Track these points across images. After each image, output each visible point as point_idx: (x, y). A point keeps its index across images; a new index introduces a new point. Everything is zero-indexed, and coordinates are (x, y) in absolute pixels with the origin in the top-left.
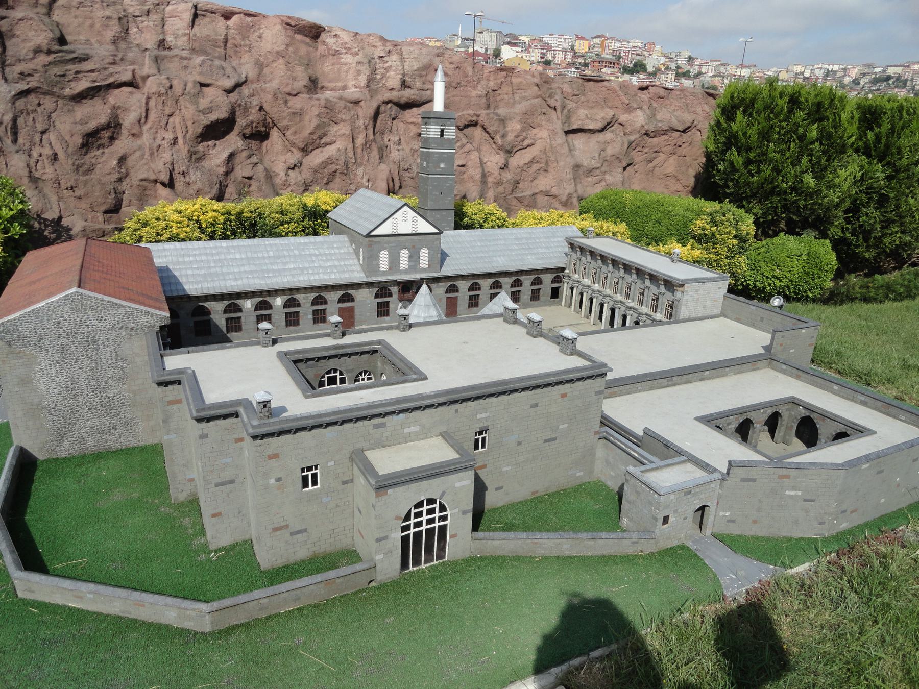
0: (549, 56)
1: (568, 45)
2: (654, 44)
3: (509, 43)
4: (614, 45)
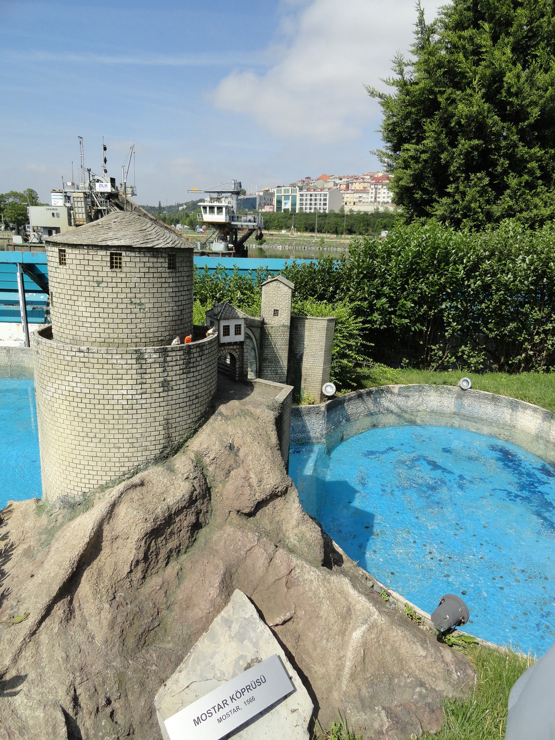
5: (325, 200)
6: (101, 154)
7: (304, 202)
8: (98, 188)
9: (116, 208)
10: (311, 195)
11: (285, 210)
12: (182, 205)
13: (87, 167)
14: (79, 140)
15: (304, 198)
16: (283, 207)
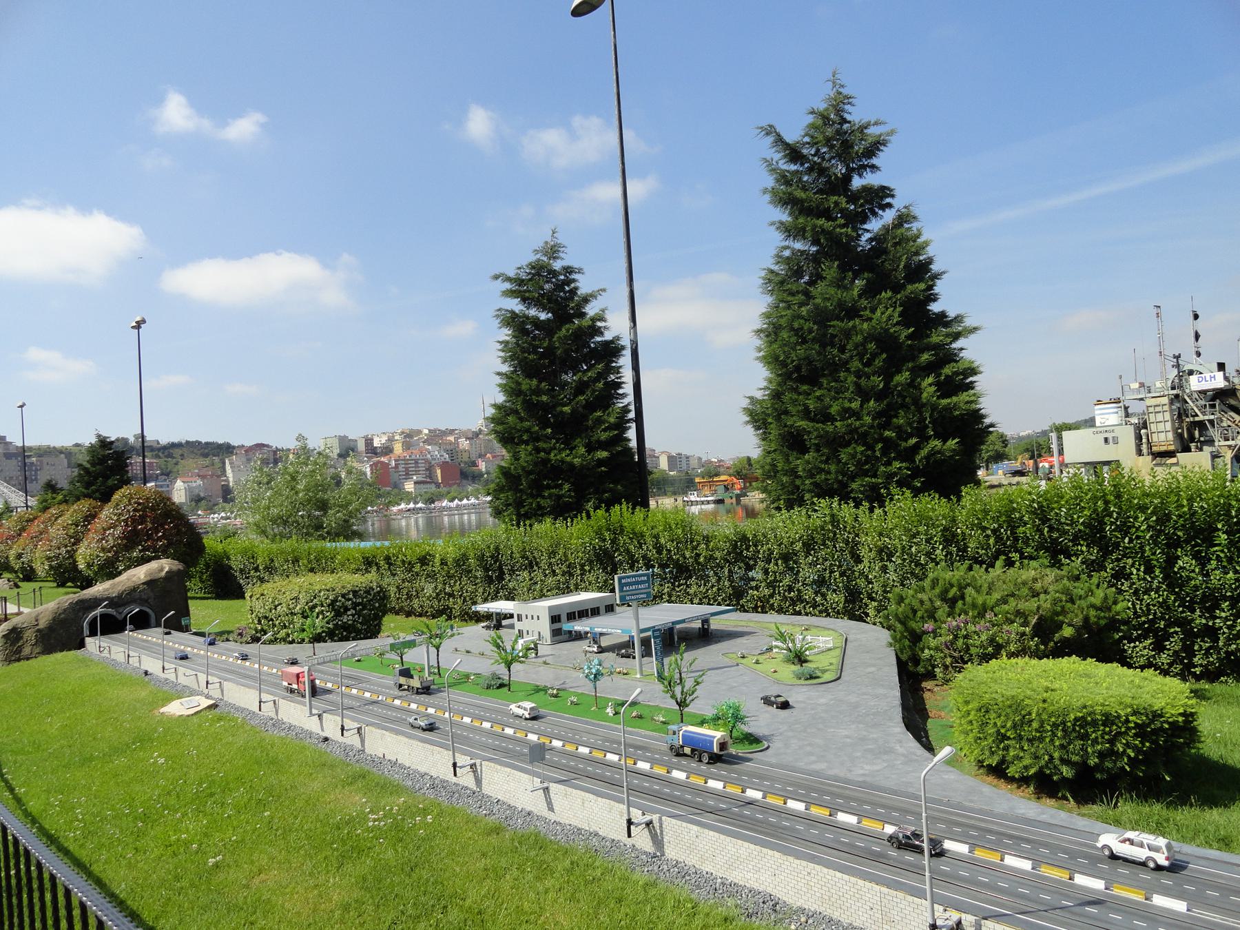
6: (1189, 326)
8: (1195, 384)
9: (1232, 414)
13: (1170, 352)
14: (1155, 311)
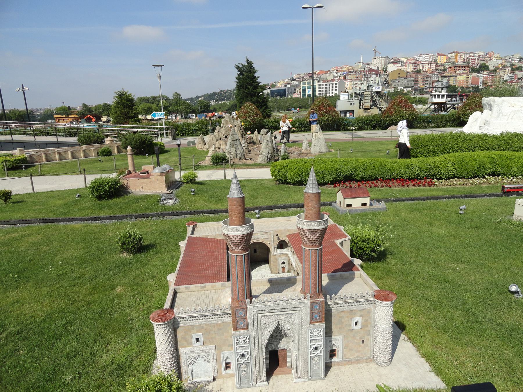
0: (420, 67)
1: (432, 59)
2: (493, 52)
3: (393, 63)
4: (464, 56)
5: (336, 87)
7: (322, 90)
10: (326, 85)
11: (309, 96)
12: (200, 97)
15: (322, 87)
16: (307, 94)
